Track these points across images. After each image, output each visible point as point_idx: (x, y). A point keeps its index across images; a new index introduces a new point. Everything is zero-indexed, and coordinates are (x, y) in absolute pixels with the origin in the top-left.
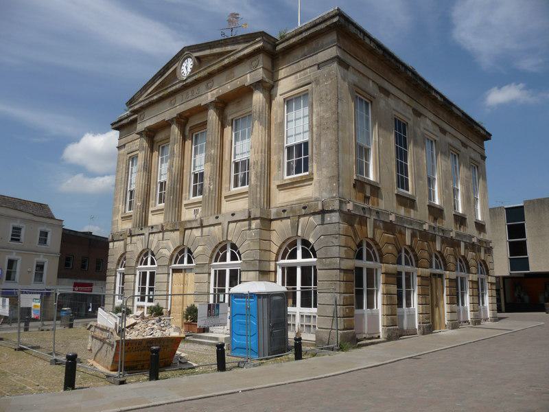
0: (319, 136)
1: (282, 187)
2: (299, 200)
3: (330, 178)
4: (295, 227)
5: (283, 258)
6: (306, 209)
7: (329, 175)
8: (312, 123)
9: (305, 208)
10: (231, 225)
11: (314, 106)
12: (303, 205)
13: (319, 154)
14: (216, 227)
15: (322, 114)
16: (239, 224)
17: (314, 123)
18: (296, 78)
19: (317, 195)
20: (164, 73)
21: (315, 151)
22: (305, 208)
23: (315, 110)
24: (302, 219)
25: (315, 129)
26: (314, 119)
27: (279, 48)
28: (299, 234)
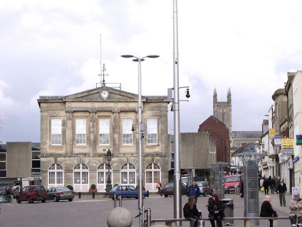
0: (162, 134)
1: (148, 147)
2: (155, 152)
3: (165, 147)
4: (153, 160)
5: (147, 168)
6: (157, 154)
7: (165, 146)
8: (159, 129)
9: (157, 155)
10: (131, 157)
11: (160, 124)
12: (156, 154)
13: (162, 139)
14: (124, 158)
15: (163, 127)
16: (134, 158)
17: (160, 129)
18: (152, 112)
19: (161, 151)
20: (90, 92)
21: (160, 138)
22: (157, 155)
23: (160, 125)
24: (155, 158)
25: (160, 131)
26: (159, 128)
27: (148, 101)
28: (155, 162)
